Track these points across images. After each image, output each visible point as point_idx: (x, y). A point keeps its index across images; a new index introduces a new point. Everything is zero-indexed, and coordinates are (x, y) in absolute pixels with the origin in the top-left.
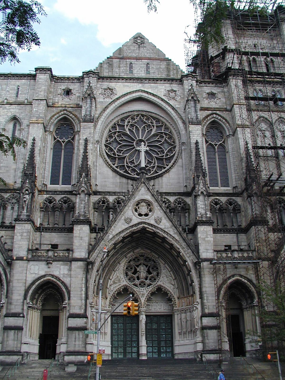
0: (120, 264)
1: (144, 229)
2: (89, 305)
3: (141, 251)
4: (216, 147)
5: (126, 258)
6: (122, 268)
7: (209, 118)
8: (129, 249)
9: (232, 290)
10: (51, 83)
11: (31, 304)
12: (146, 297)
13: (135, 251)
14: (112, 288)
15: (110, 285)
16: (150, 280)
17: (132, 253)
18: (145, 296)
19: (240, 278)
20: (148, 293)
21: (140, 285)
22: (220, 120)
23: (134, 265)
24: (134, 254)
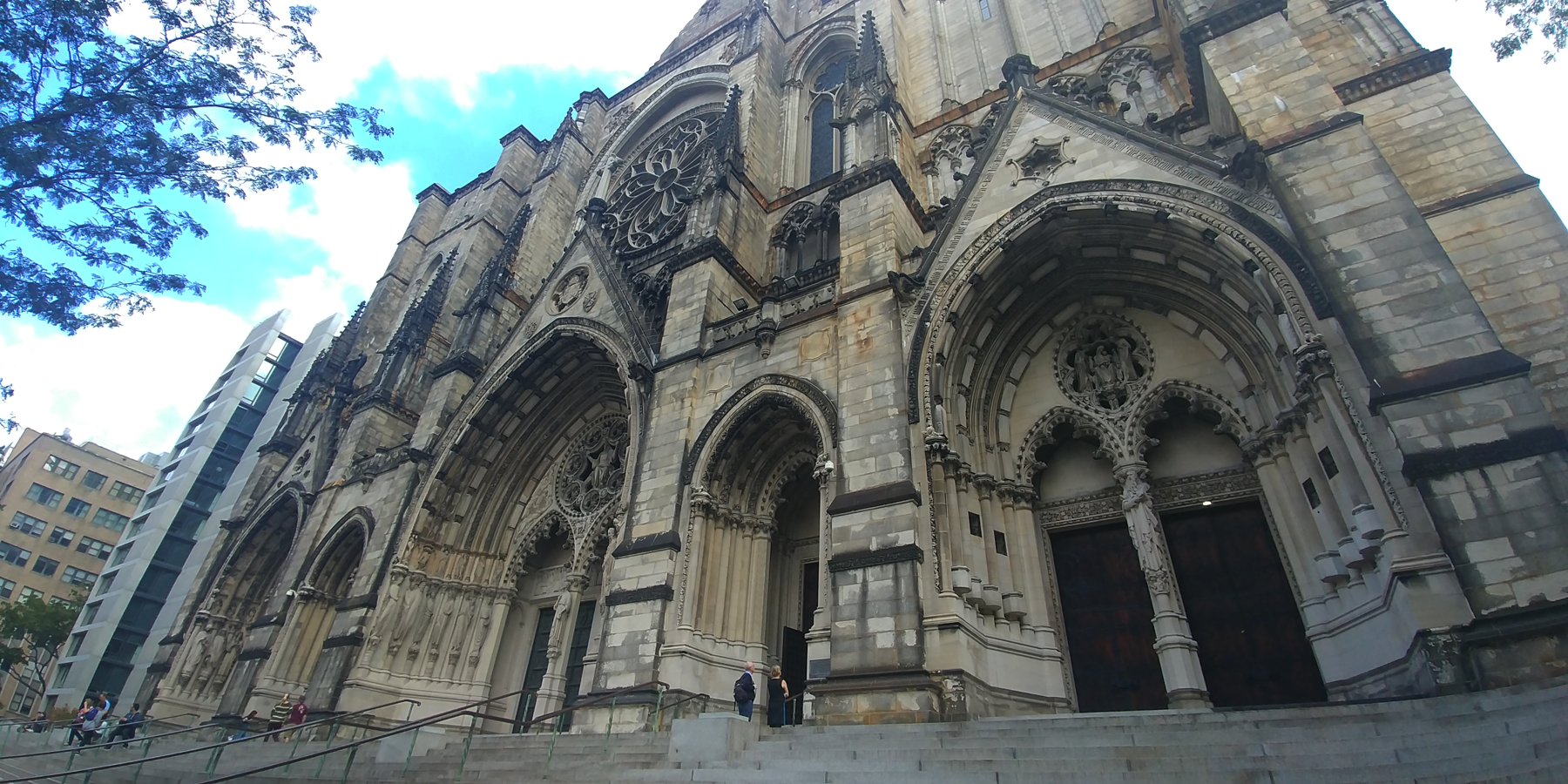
0: (553, 460)
1: (557, 334)
2: (390, 569)
3: (605, 413)
4: (834, 97)
5: (568, 439)
6: (557, 468)
7: (811, 41)
8: (570, 412)
9: (798, 452)
10: (537, 157)
11: (308, 590)
12: (589, 535)
13: (589, 415)
14: (523, 525)
15: (520, 520)
16: (614, 485)
17: (580, 424)
18: (586, 535)
19: (774, 388)
20: (596, 523)
21: (589, 504)
22: (840, 29)
23: (588, 453)
24: (589, 425)
